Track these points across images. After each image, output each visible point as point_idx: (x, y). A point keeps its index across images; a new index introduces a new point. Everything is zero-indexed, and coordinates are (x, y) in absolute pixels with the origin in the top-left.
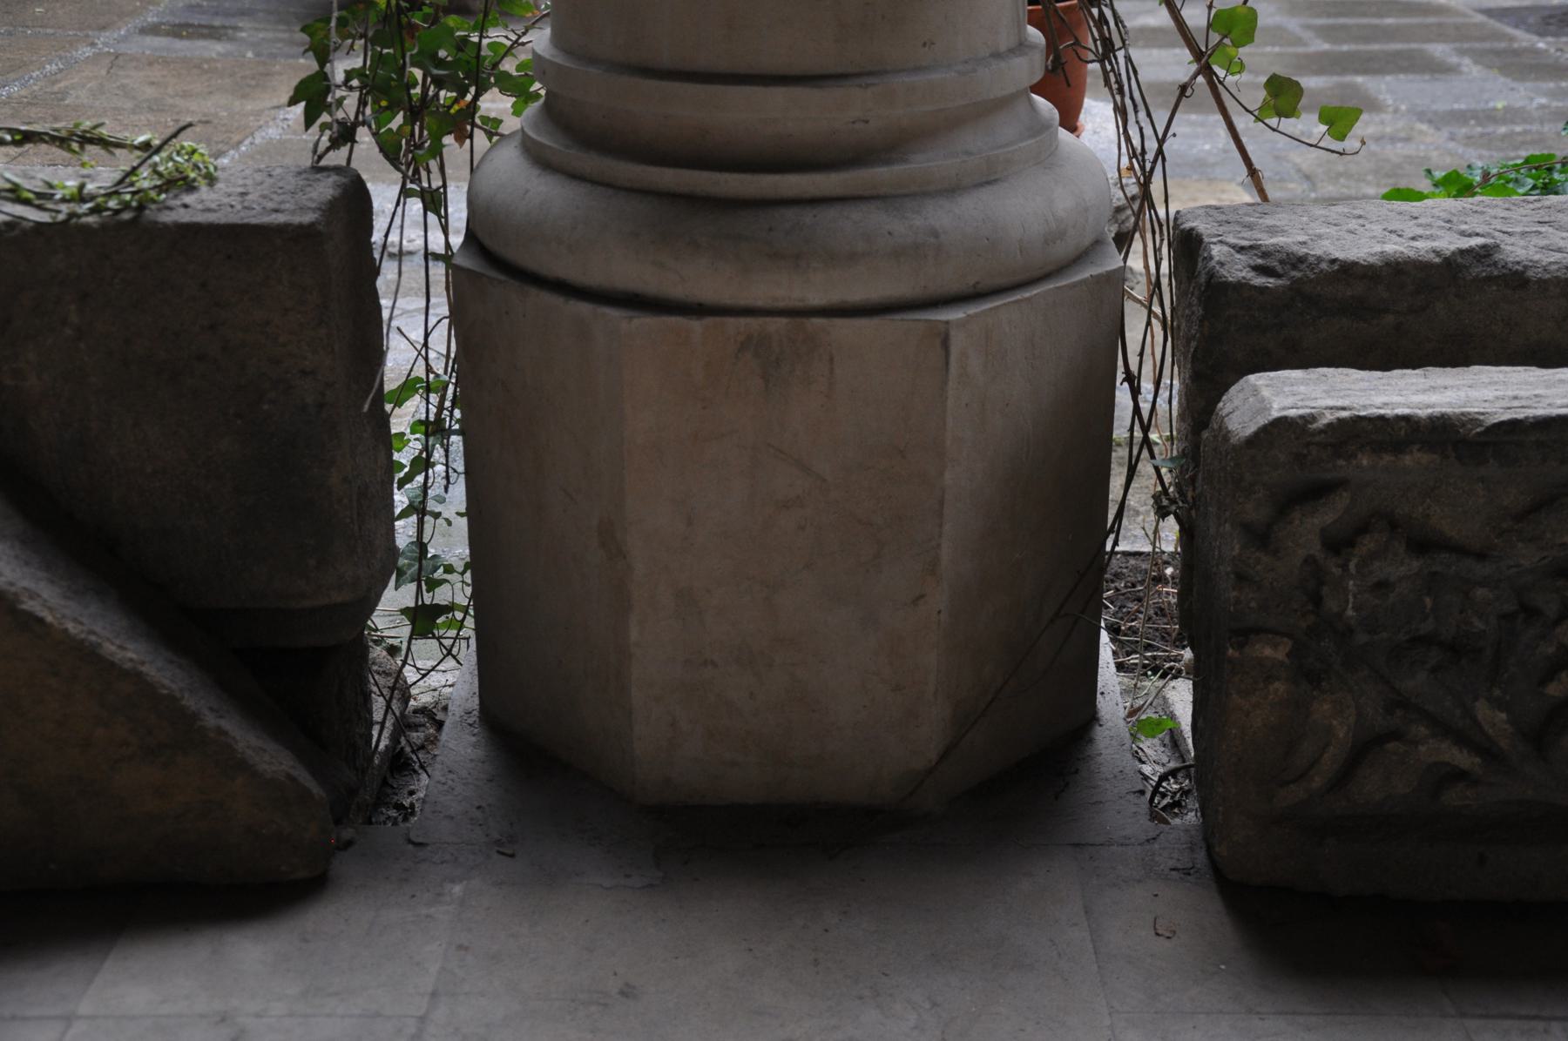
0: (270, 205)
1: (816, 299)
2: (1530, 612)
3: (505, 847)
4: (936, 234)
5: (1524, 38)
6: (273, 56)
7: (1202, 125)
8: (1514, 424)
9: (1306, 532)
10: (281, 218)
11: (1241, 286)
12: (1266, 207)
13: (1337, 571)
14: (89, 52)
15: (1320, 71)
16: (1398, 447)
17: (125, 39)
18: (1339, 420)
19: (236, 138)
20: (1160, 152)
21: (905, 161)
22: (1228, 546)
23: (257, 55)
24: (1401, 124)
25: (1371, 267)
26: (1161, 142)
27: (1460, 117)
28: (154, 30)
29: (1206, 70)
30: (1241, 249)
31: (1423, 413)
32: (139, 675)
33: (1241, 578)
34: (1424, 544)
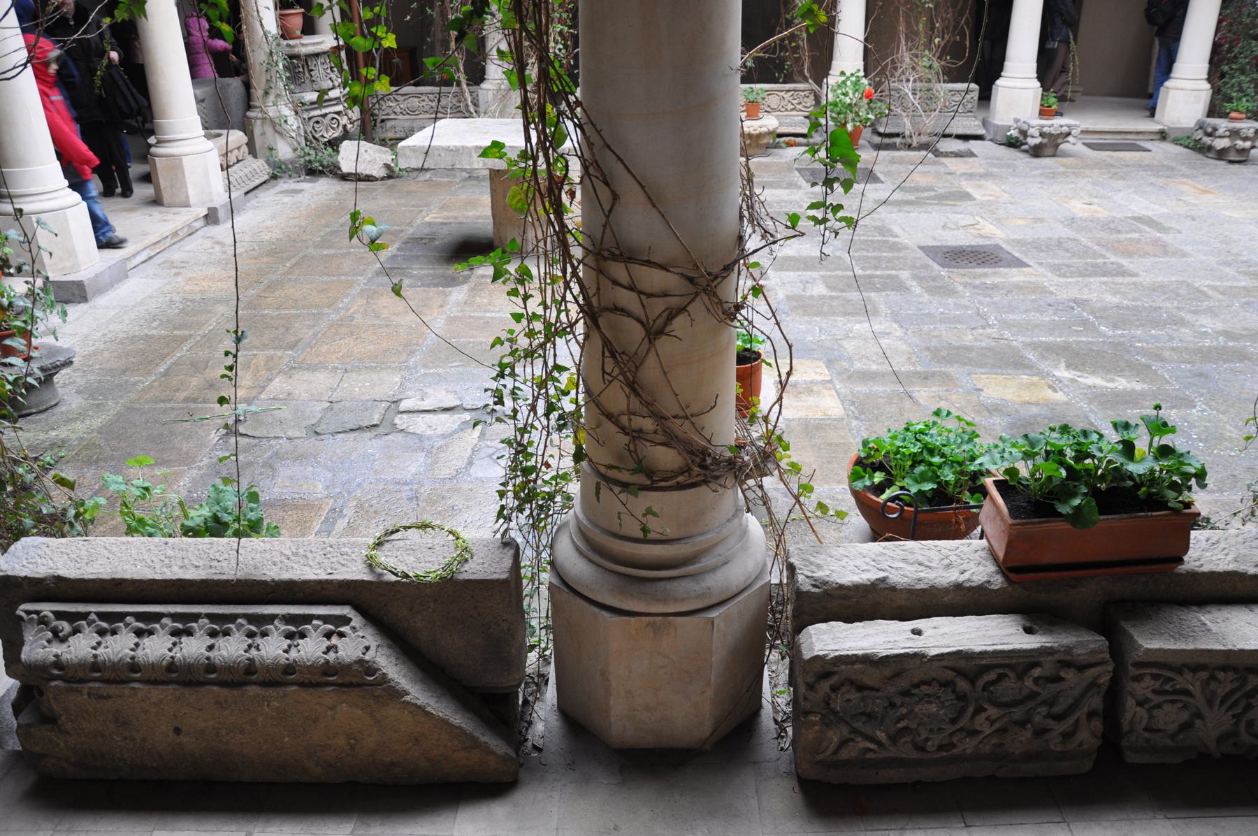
2: (892, 705)
3: (571, 766)
7: (810, 323)
9: (825, 686)
10: (496, 577)
11: (808, 592)
16: (853, 663)
22: (802, 690)
31: (860, 653)
32: (460, 728)
33: (805, 698)
34: (861, 688)
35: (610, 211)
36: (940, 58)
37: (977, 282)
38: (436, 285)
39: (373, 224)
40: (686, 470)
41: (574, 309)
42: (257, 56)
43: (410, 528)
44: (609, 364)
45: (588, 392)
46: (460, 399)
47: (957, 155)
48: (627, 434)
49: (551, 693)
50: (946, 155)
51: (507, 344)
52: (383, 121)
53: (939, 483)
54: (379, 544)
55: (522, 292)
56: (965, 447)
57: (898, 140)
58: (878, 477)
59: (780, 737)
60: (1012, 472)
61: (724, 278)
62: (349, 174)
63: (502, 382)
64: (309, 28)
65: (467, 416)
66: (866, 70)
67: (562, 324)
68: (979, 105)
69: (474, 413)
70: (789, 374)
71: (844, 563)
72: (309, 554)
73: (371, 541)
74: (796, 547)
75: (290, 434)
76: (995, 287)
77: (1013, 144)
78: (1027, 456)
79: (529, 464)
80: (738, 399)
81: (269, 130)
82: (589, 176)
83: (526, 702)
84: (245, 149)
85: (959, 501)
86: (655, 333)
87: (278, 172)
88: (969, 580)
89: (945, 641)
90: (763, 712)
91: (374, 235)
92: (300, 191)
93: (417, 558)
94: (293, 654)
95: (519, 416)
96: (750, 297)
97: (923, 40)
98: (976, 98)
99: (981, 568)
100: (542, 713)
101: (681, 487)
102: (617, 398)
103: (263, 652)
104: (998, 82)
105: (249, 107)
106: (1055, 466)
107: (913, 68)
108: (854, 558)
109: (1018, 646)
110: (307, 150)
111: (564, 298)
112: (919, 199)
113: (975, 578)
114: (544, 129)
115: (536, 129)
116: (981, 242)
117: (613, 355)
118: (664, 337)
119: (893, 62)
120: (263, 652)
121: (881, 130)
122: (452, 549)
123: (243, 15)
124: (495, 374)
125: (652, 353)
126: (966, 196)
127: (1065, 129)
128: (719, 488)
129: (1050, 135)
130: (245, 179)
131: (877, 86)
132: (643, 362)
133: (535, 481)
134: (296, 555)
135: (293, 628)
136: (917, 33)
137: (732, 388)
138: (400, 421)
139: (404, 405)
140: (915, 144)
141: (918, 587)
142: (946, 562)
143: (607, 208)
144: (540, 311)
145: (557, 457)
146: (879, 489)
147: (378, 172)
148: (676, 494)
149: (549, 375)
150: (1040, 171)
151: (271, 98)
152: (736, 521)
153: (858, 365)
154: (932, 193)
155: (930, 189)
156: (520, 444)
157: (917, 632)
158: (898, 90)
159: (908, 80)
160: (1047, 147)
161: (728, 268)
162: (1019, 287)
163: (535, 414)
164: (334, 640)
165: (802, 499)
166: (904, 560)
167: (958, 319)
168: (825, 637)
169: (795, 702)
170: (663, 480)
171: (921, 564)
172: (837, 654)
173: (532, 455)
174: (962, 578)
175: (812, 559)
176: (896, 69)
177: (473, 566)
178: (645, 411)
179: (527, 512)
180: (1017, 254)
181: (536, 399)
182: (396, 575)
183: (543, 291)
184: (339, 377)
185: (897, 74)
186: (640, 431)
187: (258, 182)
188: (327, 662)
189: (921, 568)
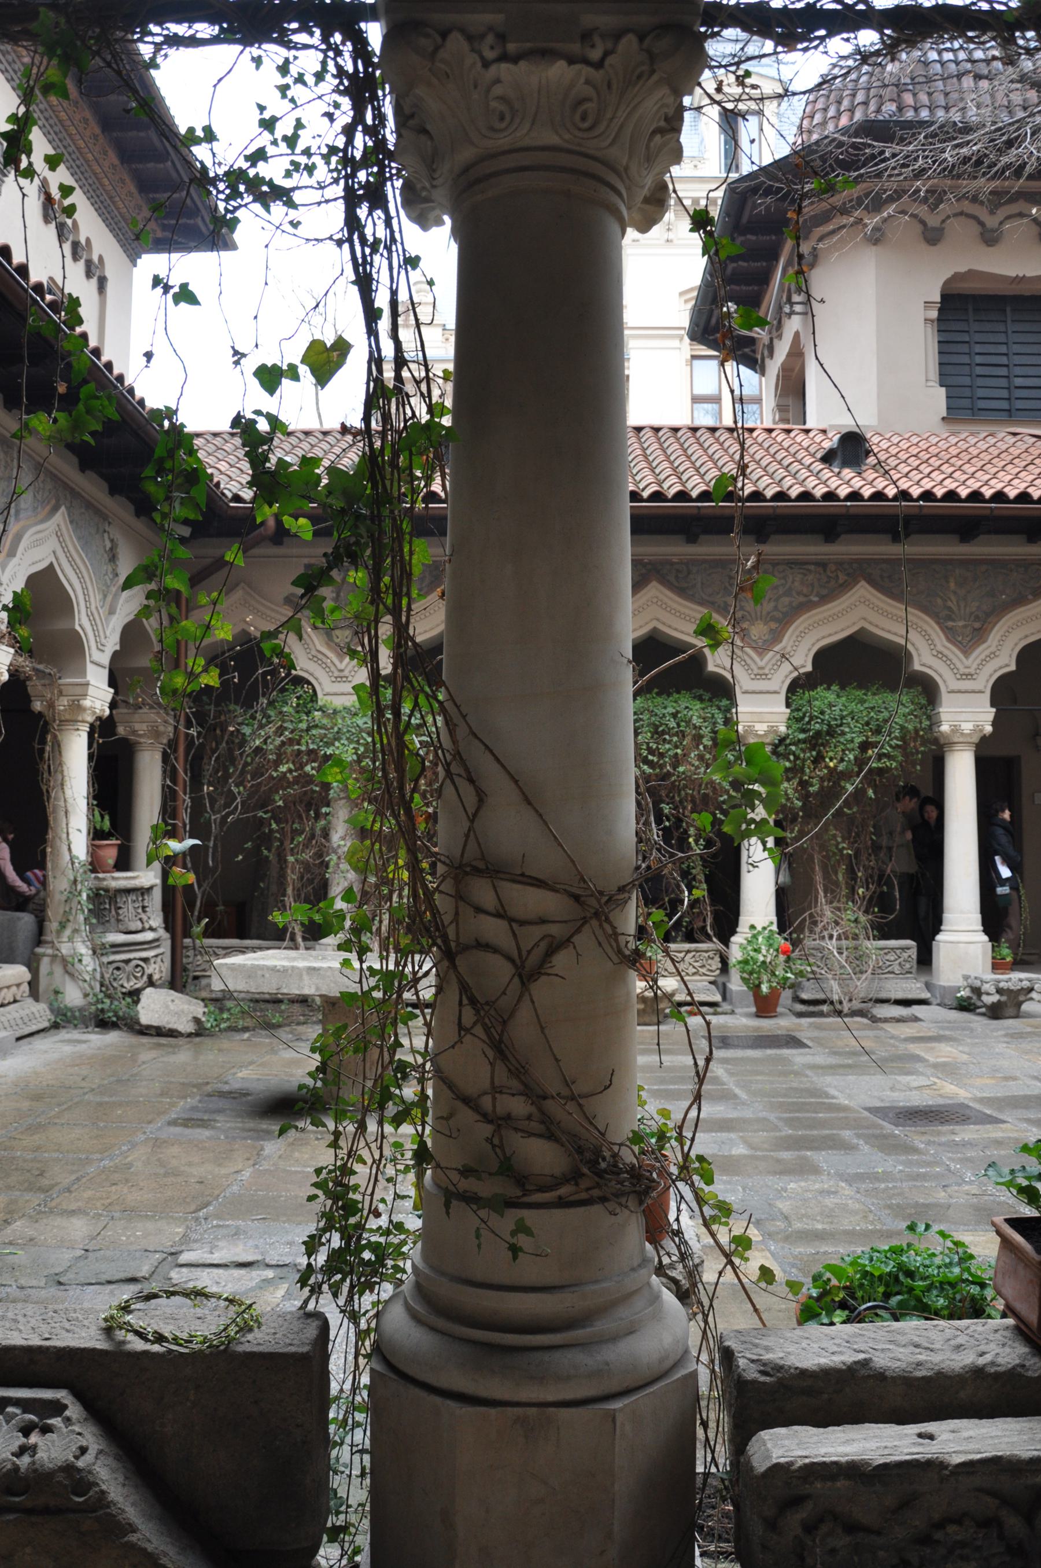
0: (288, 1341)
4: (607, 1364)
5: (888, 1128)
6: (234, 1138)
7: (729, 1183)
8: (885, 1466)
9: (794, 1520)
11: (754, 1382)
12: (764, 1331)
13: (810, 1543)
14: (143, 1137)
15: (788, 1149)
17: (160, 1129)
18: (806, 1465)
19: (216, 1192)
20: (711, 1305)
21: (592, 1326)
23: (227, 1137)
24: (832, 1183)
25: (814, 1371)
26: (711, 1301)
27: (860, 1177)
28: (173, 1123)
29: (731, 1263)
30: (753, 1361)
31: (843, 1460)
35: (475, 815)
36: (866, 912)
37: (943, 1139)
40: (574, 1176)
42: (59, 884)
44: (469, 1016)
46: (262, 1254)
48: (490, 1122)
50: (886, 1020)
52: (196, 978)
57: (825, 1008)
62: (149, 1027)
64: (124, 863)
65: (270, 1274)
66: (779, 927)
68: (918, 969)
69: (279, 1270)
70: (708, 1060)
71: (804, 1345)
72: (20, 1318)
76: (965, 1144)
77: (965, 1006)
81: (58, 970)
84: (25, 987)
86: (528, 973)
87: (62, 1020)
88: (993, 1363)
89: (972, 1446)
92: (85, 1042)
95: (342, 1142)
97: (845, 891)
98: (914, 956)
99: (1007, 1350)
101: (563, 1203)
102: (476, 1070)
104: (938, 937)
105: (39, 942)
107: (837, 923)
110: (101, 996)
113: (1000, 1360)
116: (941, 1101)
117: (473, 1002)
118: (543, 978)
119: (811, 916)
121: (804, 996)
123: (50, 836)
125: (526, 997)
126: (918, 1059)
127: (1026, 984)
128: (618, 1210)
130: (19, 1022)
131: (796, 943)
132: (512, 1014)
136: (837, 884)
139: (184, 1258)
140: (846, 1010)
141: (919, 1374)
143: (471, 811)
147: (185, 1026)
148: (558, 1214)
151: (68, 932)
153: (798, 1225)
158: (821, 949)
159: (831, 937)
160: (1005, 1007)
165: (737, 1261)
167: (923, 1177)
170: (542, 1189)
171: (917, 1346)
172: (807, 1461)
174: (981, 1361)
176: (815, 923)
178: (515, 1083)
180: (988, 1112)
184: (101, 1225)
185: (818, 930)
186: (508, 1117)
187: (34, 1028)
188: (16, 1469)
189: (918, 1350)
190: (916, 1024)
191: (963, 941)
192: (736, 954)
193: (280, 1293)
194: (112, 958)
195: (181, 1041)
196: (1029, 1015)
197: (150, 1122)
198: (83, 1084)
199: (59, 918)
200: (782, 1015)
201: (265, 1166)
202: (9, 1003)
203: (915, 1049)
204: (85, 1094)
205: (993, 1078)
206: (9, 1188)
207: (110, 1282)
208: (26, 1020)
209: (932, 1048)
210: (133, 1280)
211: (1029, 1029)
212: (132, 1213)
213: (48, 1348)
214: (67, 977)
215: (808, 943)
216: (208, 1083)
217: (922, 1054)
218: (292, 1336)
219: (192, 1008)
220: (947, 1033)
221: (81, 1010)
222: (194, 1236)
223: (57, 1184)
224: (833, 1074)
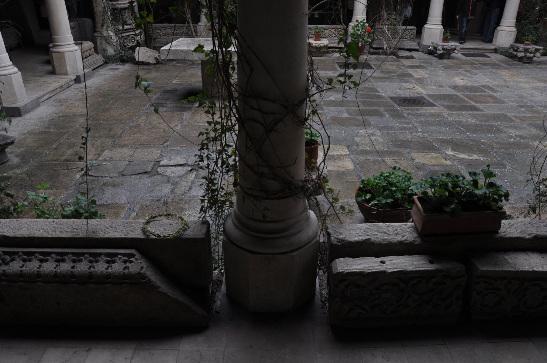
1: (275, 252)
10: (199, 237)
11: (336, 245)
18: (347, 273)
19: (170, 135)
27: (384, 128)
29: (332, 205)
30: (336, 238)
37: (414, 113)
38: (177, 111)
39: (146, 81)
41: (234, 119)
43: (162, 215)
45: (240, 156)
47: (407, 57)
49: (223, 287)
51: (205, 135)
52: (155, 39)
53: (395, 199)
54: (148, 223)
55: (211, 112)
56: (406, 183)
57: (381, 51)
58: (368, 196)
59: (323, 308)
60: (425, 193)
61: (300, 106)
63: (203, 151)
67: (229, 126)
70: (328, 149)
72: (117, 226)
73: (144, 221)
74: (331, 227)
75: (111, 175)
78: (432, 186)
79: (214, 188)
80: (306, 159)
81: (104, 42)
82: (241, 60)
83: (213, 292)
84: (93, 50)
85: (403, 206)
87: (108, 60)
88: (406, 240)
89: (395, 266)
90: (316, 297)
91: (146, 86)
92: (118, 69)
93: (164, 228)
94: (110, 270)
95: (210, 167)
96: (311, 115)
99: (411, 235)
100: (220, 297)
101: (280, 198)
103: (96, 269)
104: (425, 26)
105: (95, 31)
106: (444, 190)
108: (356, 230)
109: (426, 269)
110: (121, 51)
111: (230, 114)
112: (388, 76)
113: (408, 239)
114: (221, 40)
115: (218, 40)
116: (416, 95)
119: (379, 16)
120: (96, 269)
121: (374, 46)
122: (180, 225)
124: (199, 148)
126: (410, 76)
127: (453, 47)
129: (447, 50)
130: (93, 63)
131: (372, 27)
133: (217, 195)
134: (111, 227)
135: (109, 259)
137: (303, 155)
138: (160, 170)
139: (162, 163)
141: (384, 243)
142: (396, 232)
144: (220, 120)
145: (226, 184)
146: (369, 201)
147: (152, 61)
149: (223, 149)
150: (442, 65)
151: (105, 27)
152: (304, 213)
153: (361, 148)
154: (395, 74)
155: (395, 72)
156: (210, 179)
157: (383, 262)
159: (386, 25)
161: (302, 102)
162: (432, 115)
163: (217, 165)
164: (128, 264)
166: (378, 231)
168: (343, 264)
169: (329, 293)
171: (385, 233)
173: (216, 184)
174: (403, 239)
175: (338, 230)
176: (380, 19)
177: (189, 232)
179: (214, 209)
180: (431, 101)
181: (217, 159)
182: (155, 236)
183: (221, 112)
184: (133, 151)
185: (381, 22)
187: (98, 65)
190: (412, 60)
191: (434, 28)
192: (350, 30)
193: (193, 176)
194: (123, 35)
195: (152, 67)
196: (453, 58)
197: (144, 106)
198: (119, 89)
199: (101, 22)
200: (365, 53)
201: (185, 123)
202: (88, 57)
203: (411, 71)
204: (120, 94)
205: (435, 86)
206: (101, 137)
207: (139, 174)
208: (95, 62)
209: (416, 71)
210: (146, 173)
211: (452, 65)
212: (143, 145)
213: (127, 238)
214: (107, 45)
215: (377, 26)
216: (163, 87)
217: (412, 74)
218: (199, 232)
219: (154, 54)
220: (423, 64)
221: (114, 56)
222: (164, 154)
223: (116, 134)
224: (380, 82)
